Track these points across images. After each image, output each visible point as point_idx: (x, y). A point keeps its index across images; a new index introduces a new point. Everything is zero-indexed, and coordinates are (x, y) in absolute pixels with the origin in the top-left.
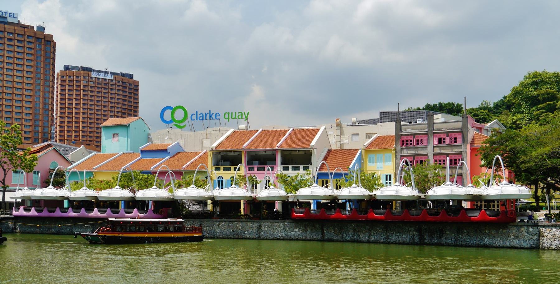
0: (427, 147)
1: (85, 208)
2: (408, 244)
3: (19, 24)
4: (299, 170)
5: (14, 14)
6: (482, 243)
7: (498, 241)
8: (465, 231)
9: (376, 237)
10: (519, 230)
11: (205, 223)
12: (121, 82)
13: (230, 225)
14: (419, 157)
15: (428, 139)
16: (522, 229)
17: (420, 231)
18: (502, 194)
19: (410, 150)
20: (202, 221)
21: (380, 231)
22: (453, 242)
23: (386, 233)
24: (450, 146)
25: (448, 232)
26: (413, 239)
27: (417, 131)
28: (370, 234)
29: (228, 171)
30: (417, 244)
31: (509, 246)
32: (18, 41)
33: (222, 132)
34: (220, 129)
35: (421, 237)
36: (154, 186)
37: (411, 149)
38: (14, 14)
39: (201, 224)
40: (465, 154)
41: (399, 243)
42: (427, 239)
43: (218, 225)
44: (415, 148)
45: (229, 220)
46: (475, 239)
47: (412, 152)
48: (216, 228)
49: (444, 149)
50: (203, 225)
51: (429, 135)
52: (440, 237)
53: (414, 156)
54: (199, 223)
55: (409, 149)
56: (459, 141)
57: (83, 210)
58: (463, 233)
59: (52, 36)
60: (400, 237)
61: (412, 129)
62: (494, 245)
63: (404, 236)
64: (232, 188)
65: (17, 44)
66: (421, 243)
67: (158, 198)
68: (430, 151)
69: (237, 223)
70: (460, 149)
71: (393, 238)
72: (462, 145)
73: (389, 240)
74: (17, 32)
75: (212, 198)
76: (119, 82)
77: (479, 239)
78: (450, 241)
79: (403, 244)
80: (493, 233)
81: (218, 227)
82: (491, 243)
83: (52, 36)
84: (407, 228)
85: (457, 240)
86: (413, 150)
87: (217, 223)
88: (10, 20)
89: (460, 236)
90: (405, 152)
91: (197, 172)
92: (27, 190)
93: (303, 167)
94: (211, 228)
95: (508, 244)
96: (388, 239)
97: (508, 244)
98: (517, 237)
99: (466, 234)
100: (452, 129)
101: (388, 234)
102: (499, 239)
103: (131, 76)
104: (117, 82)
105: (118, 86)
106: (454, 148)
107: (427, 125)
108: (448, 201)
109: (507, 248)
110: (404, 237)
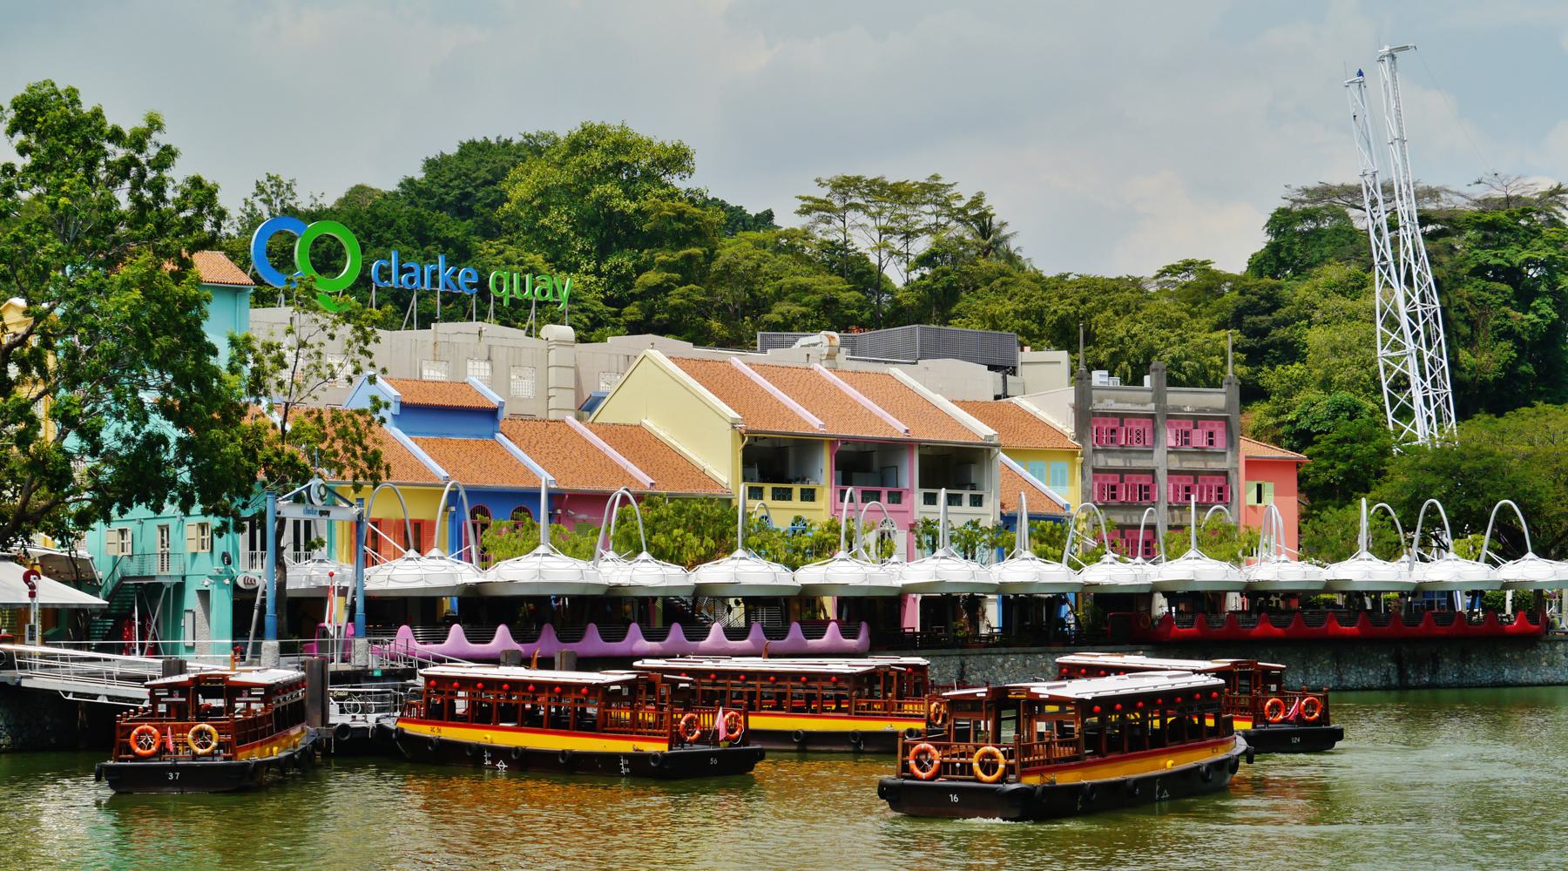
0: (1152, 452)
1: (507, 624)
2: (1379, 689)
4: (960, 504)
6: (1501, 679)
7: (1525, 675)
8: (1474, 656)
9: (1318, 678)
10: (1552, 649)
11: (972, 659)
13: (1028, 662)
14: (1134, 476)
15: (1154, 431)
16: (1558, 648)
17: (1398, 659)
18: (542, 580)
19: (1112, 457)
20: (963, 655)
21: (1325, 662)
22: (1456, 680)
23: (1338, 668)
24: (1201, 452)
25: (1446, 660)
26: (1387, 677)
27: (1136, 408)
28: (1306, 672)
29: (784, 499)
30: (1395, 688)
31: (1541, 681)
33: (491, 341)
34: (480, 332)
35: (1402, 674)
36: (842, 552)
37: (1114, 454)
39: (963, 665)
40: (1235, 476)
41: (1364, 689)
42: (1412, 676)
43: (1002, 666)
44: (1124, 451)
45: (1026, 649)
46: (1490, 672)
47: (1116, 462)
48: (997, 674)
49: (1189, 460)
50: (968, 667)
51: (1158, 421)
52: (1434, 672)
53: (1122, 472)
54: (958, 662)
55: (1110, 454)
56: (1220, 444)
57: (593, 631)
58: (1470, 660)
60: (1363, 675)
61: (1117, 401)
62: (1519, 681)
63: (1371, 673)
64: (935, 558)
66: (1403, 687)
67: (1116, 586)
68: (1161, 460)
69: (1040, 656)
70: (1220, 461)
71: (1352, 678)
72: (1229, 454)
73: (1343, 684)
75: (1000, 589)
77: (1495, 672)
78: (1451, 677)
79: (1370, 689)
80: (1516, 657)
81: (1000, 670)
82: (1515, 679)
84: (1375, 654)
85: (1462, 675)
86: (1119, 457)
87: (1000, 660)
89: (1467, 666)
90: (1102, 461)
92: (1286, 561)
93: (773, 489)
94: (987, 674)
95: (1539, 677)
96: (1342, 680)
97: (1538, 678)
98: (1551, 664)
99: (1475, 661)
100: (1205, 411)
101: (1341, 669)
102: (1526, 669)
106: (1209, 457)
107: (1150, 394)
108: (655, 599)
109: (1539, 685)
110: (1371, 676)
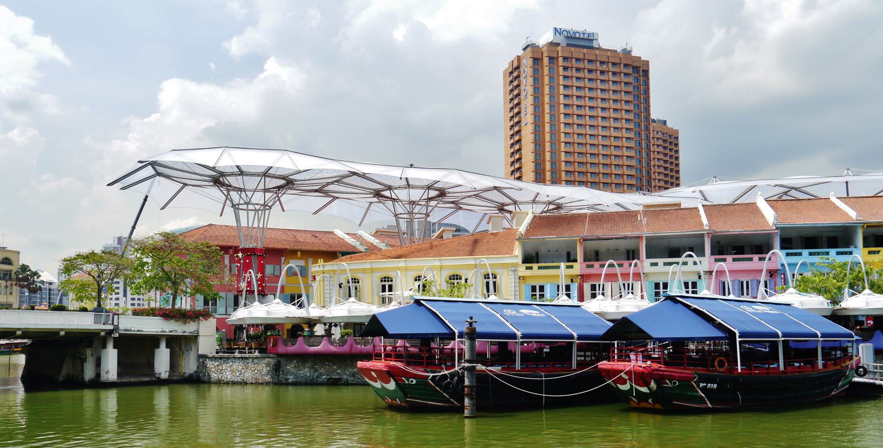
3: (600, 49)
5: (593, 33)
12: (660, 133)
32: (614, 74)
38: (593, 33)
59: (648, 61)
65: (612, 78)
74: (611, 60)
76: (657, 132)
83: (648, 61)
88: (595, 45)
91: (606, 275)
103: (665, 122)
104: (655, 132)
105: (658, 139)
